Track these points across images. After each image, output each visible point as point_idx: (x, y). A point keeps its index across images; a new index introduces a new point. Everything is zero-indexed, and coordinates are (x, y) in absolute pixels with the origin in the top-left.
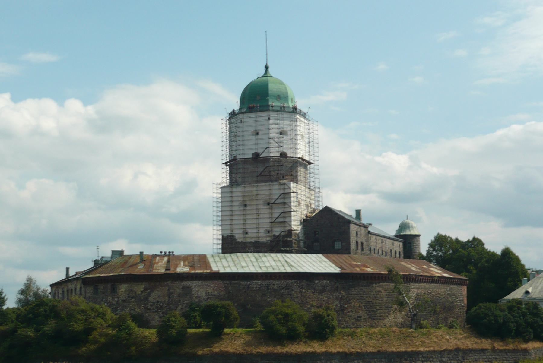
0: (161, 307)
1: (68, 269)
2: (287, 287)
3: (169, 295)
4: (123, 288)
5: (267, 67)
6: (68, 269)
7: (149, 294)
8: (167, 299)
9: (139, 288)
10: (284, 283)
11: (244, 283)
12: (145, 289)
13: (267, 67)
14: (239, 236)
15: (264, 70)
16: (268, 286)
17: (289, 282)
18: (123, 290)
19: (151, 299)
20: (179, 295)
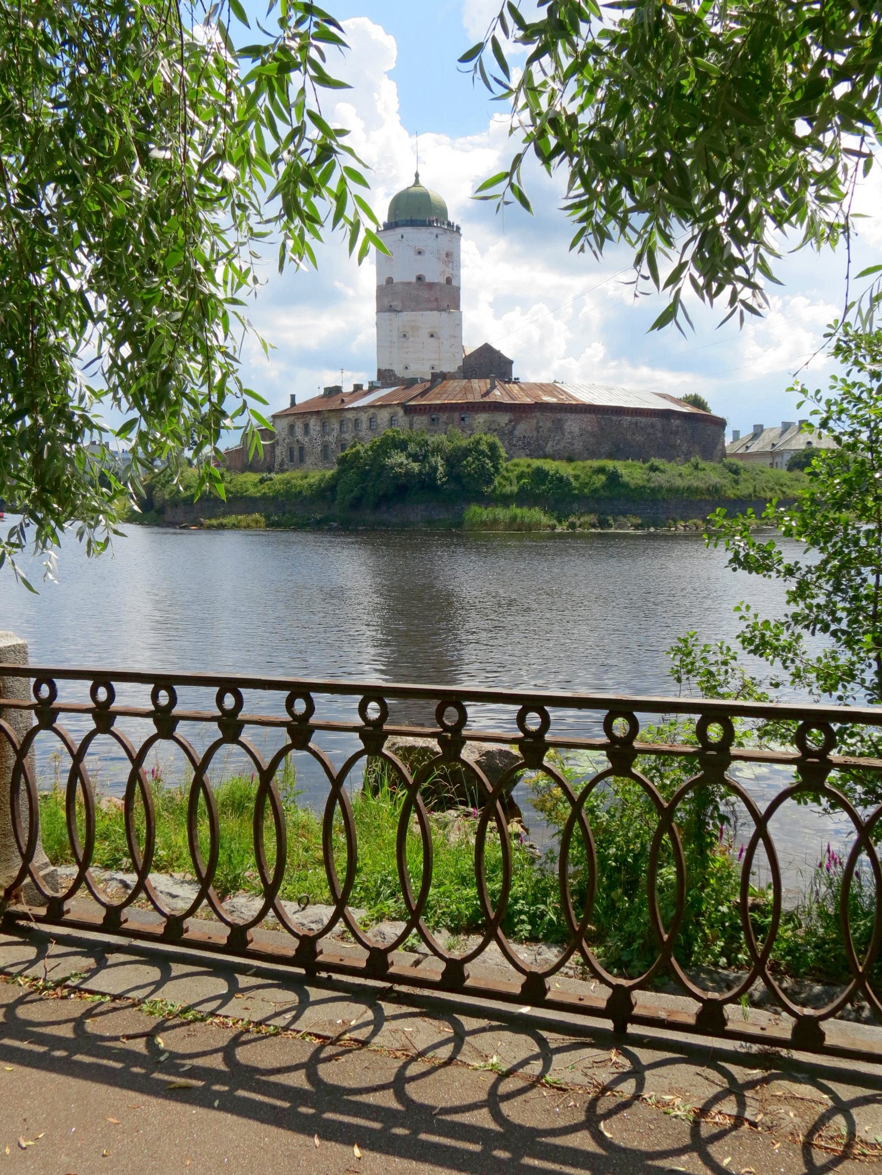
0: (529, 443)
1: (293, 397)
2: (653, 426)
3: (538, 429)
4: (481, 418)
5: (417, 175)
6: (293, 397)
7: (514, 428)
8: (535, 434)
9: (503, 419)
10: (643, 420)
11: (614, 418)
12: (510, 421)
13: (417, 175)
14: (399, 372)
15: (414, 179)
16: (636, 423)
17: (654, 419)
18: (481, 421)
19: (516, 433)
20: (549, 430)
